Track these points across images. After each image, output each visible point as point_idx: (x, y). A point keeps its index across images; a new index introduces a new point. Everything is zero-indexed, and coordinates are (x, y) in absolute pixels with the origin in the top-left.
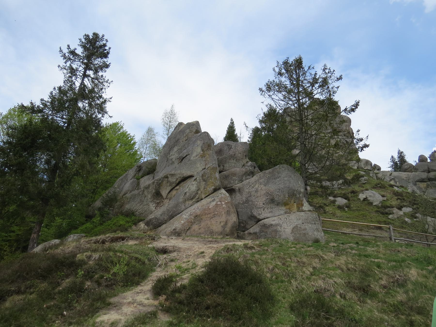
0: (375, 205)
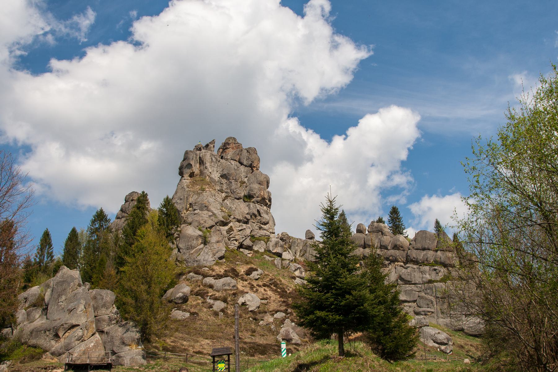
0: (251, 311)
